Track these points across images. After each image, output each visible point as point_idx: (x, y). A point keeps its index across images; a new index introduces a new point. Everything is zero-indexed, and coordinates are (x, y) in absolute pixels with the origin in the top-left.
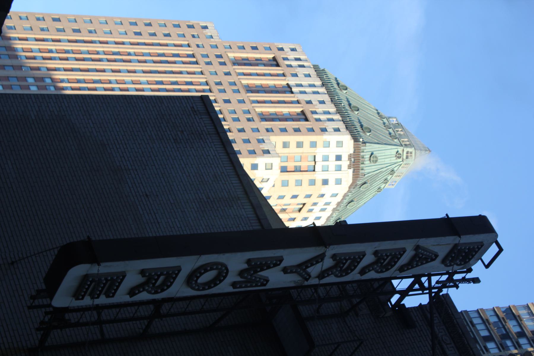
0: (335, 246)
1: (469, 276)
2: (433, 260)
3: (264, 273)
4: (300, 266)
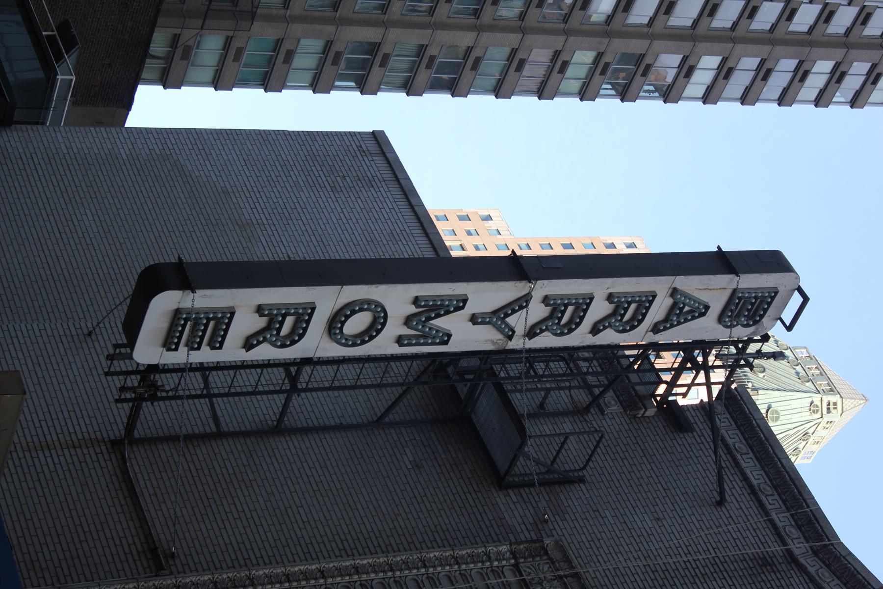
0: (546, 282)
1: (768, 347)
2: (702, 315)
4: (495, 312)
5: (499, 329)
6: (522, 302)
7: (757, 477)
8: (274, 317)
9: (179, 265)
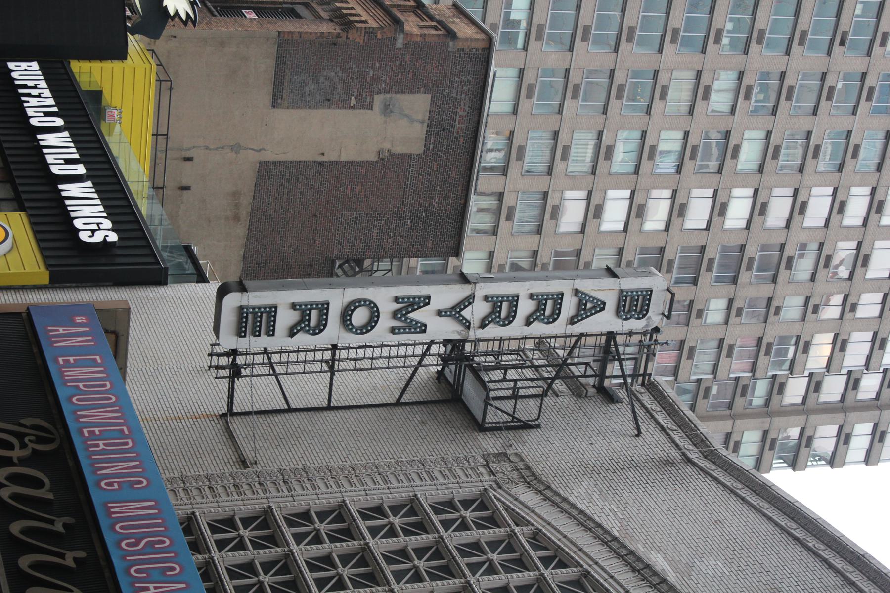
2: (603, 309)
4: (453, 308)
6: (469, 301)
8: (303, 310)
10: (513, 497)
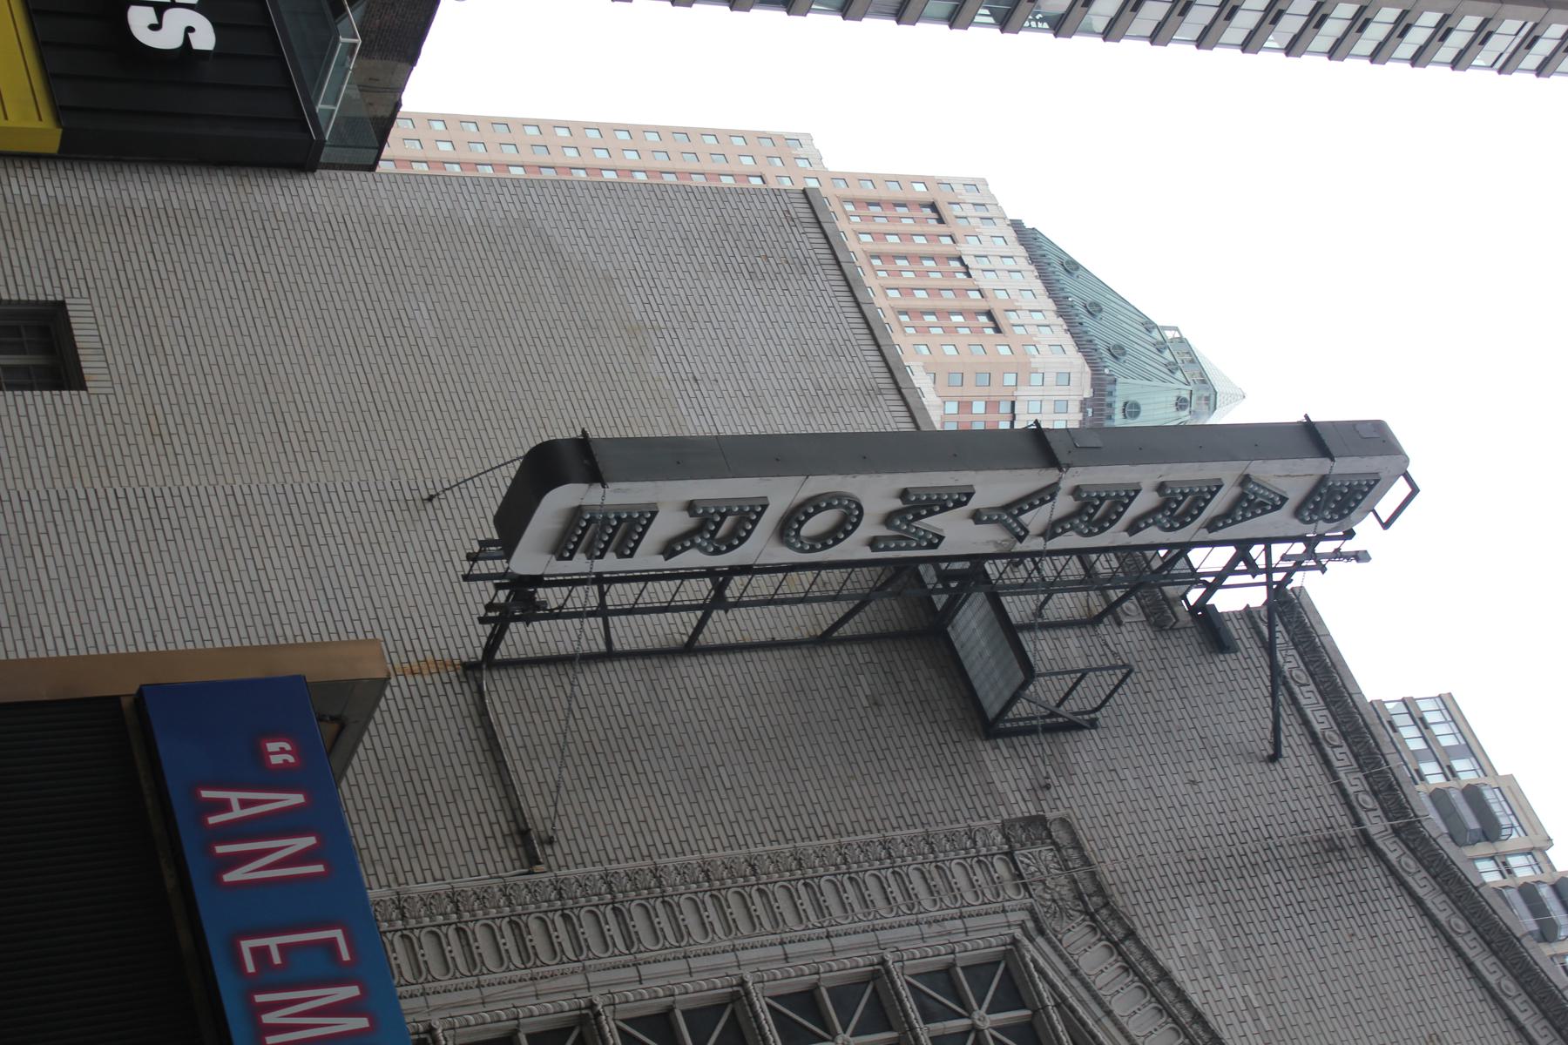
0: (1080, 469)
1: (1348, 546)
2: (1276, 508)
3: (934, 522)
4: (1006, 508)
5: (1008, 527)
7: (1321, 720)
9: (583, 444)
10: (1068, 964)
